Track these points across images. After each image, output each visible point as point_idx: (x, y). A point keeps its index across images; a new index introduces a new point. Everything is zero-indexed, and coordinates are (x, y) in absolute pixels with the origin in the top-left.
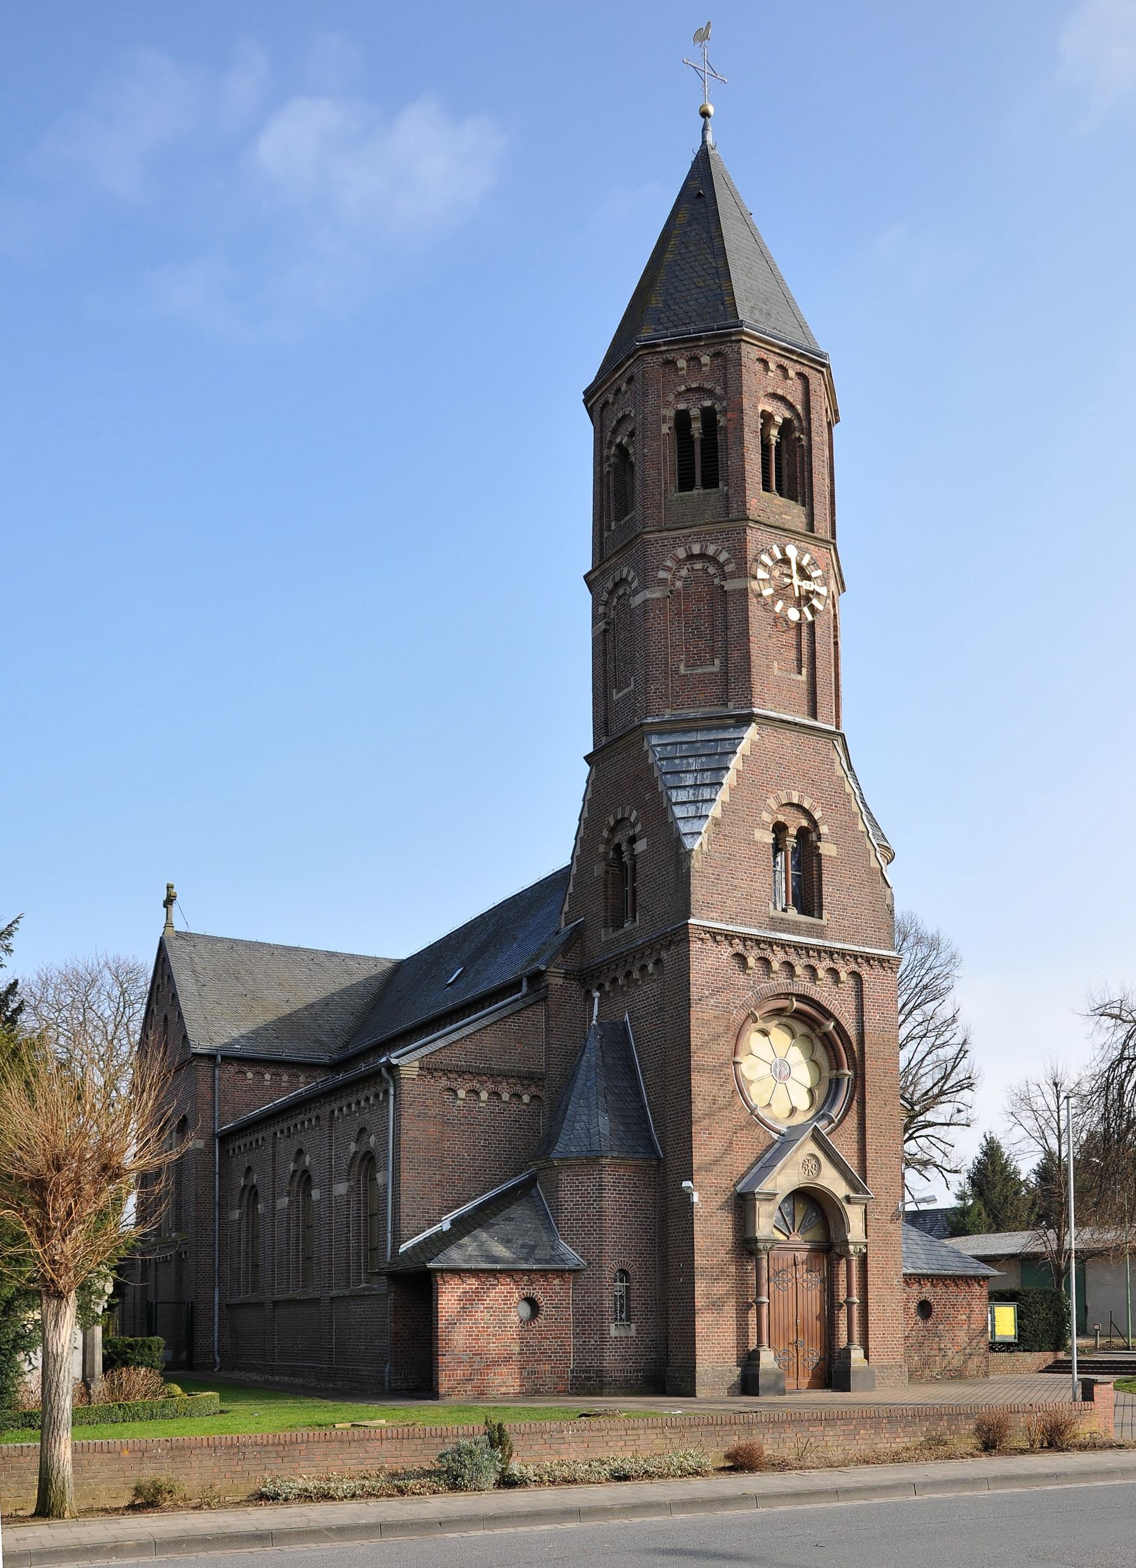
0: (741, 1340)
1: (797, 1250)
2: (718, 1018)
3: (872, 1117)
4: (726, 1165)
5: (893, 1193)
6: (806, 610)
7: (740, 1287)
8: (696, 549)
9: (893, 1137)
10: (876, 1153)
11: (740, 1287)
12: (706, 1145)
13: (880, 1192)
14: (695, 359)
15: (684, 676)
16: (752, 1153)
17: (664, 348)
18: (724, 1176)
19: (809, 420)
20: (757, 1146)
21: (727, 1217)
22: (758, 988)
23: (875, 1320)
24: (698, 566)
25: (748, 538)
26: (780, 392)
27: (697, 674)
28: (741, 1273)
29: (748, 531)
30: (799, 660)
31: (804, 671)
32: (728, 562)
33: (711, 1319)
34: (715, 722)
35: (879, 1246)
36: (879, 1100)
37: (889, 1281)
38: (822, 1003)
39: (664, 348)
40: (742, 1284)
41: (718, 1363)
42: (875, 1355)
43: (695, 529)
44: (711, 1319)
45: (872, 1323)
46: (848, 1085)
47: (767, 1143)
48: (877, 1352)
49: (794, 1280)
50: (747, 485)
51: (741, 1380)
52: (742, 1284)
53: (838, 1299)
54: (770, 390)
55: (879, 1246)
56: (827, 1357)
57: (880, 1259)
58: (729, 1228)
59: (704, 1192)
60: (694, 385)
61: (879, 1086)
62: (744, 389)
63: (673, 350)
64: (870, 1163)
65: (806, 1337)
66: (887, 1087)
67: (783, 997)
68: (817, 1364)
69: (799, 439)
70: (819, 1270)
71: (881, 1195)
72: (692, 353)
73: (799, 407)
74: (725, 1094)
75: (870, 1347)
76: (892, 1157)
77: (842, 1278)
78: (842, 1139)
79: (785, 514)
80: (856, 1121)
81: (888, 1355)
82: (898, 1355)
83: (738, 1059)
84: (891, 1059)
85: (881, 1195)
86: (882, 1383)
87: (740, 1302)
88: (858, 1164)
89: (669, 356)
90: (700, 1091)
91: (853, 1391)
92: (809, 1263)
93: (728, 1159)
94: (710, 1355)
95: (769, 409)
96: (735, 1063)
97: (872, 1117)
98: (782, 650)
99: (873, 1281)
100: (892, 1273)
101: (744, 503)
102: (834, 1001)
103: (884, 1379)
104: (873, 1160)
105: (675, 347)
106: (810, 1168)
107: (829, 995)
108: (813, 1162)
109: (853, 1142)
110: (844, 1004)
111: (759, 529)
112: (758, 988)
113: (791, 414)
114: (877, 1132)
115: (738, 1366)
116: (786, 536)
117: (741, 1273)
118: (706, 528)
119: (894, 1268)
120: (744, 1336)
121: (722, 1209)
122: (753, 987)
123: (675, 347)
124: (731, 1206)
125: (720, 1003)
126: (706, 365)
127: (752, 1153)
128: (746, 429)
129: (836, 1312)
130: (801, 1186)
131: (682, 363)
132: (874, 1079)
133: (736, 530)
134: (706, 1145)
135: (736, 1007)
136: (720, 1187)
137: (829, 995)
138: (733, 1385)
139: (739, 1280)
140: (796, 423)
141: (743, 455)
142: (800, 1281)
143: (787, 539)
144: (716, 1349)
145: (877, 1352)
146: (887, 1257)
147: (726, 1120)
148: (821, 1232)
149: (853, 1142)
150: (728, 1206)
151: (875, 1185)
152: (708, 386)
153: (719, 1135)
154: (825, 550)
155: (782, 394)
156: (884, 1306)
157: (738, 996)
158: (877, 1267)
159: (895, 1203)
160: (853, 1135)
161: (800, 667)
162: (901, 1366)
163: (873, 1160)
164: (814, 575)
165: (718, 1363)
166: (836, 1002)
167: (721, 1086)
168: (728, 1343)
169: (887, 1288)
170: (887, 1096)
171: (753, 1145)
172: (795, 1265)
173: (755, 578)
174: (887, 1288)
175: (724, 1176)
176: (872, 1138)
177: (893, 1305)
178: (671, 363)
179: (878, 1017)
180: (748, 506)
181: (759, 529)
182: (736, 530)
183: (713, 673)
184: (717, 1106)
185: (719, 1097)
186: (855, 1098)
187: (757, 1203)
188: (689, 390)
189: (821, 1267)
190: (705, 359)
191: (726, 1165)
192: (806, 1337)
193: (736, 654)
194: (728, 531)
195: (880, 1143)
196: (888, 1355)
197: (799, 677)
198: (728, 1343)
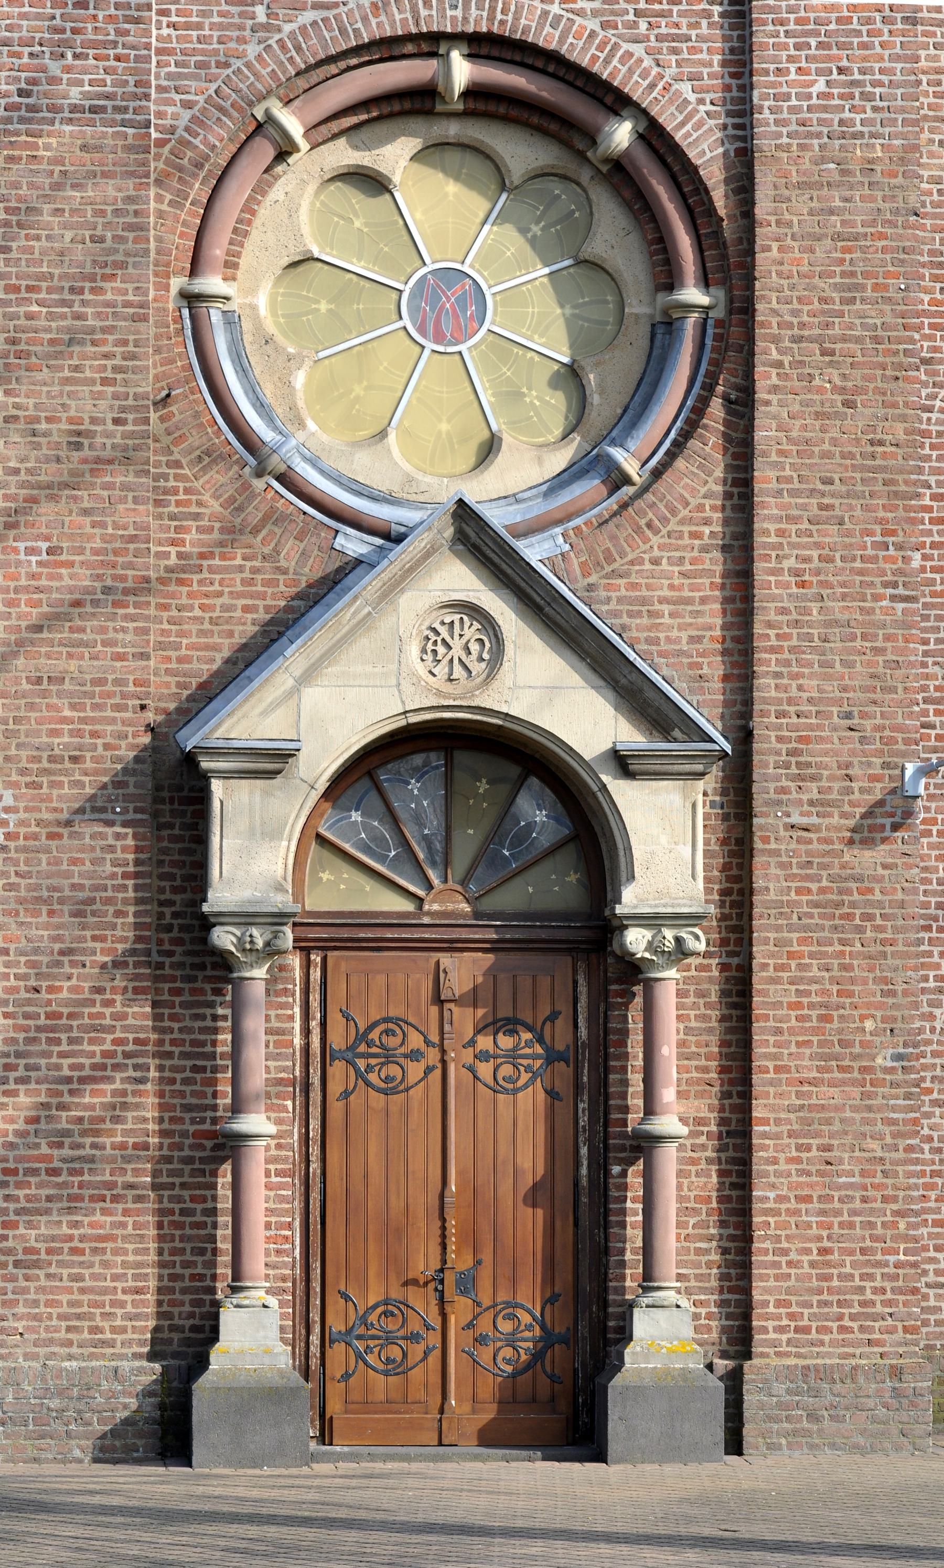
0: (186, 1265)
1: (452, 946)
2: (98, 149)
3: (781, 453)
4: (120, 657)
5: (878, 728)
7: (185, 1081)
9: (880, 521)
10: (802, 585)
11: (185, 1081)
12: (38, 590)
13: (820, 727)
16: (246, 609)
18: (110, 695)
20: (267, 583)
21: (118, 836)
22: (287, 28)
23: (780, 1199)
28: (190, 1030)
33: (45, 1192)
35: (806, 928)
36: (820, 390)
37: (854, 1057)
38: (574, 57)
40: (196, 1069)
41: (70, 1343)
42: (781, 1329)
44: (45, 1192)
45: (766, 1212)
46: (700, 346)
47: (313, 570)
48: (792, 1316)
49: (433, 1056)
51: (162, 1407)
52: (196, 1069)
53: (624, 1123)
55: (806, 928)
56: (583, 1330)
57: (815, 972)
58: (125, 876)
59: (24, 754)
61: (819, 340)
64: (770, 625)
65: (487, 1256)
66: (858, 340)
67: (410, 48)
68: (537, 1356)
70: (553, 1017)
71: (821, 740)
74: (123, 409)
75: (757, 1296)
76: (877, 598)
77: (636, 1046)
78: (655, 540)
80: (719, 473)
81: (843, 1329)
82: (891, 1331)
83: (211, 283)
84: (882, 236)
85: (821, 740)
86: (807, 1433)
87: (184, 1134)
88: (724, 627)
90: (17, 406)
91: (619, 1461)
92: (505, 993)
93: (129, 637)
94: (37, 1318)
96: (192, 299)
97: (781, 453)
99: (775, 1057)
100: (869, 1025)
102: (625, 46)
103: (813, 1417)
104: (784, 611)
106: (457, 651)
107: (604, 26)
108: (472, 631)
109: (704, 549)
110: (675, 51)
112: (287, 28)
114: (804, 507)
115: (152, 1356)
117: (190, 1030)
119: (880, 1006)
120: (202, 1252)
121: (103, 810)
122: (266, 27)
124: (138, 798)
125: (107, 97)
127: (246, 609)
129: (616, 1169)
130: (414, 719)
132: (795, 313)
134: (38, 590)
135: (187, 105)
136: (94, 734)
137: (604, 26)
138: (126, 1422)
139: (185, 1055)
142: (460, 1058)
144: (64, 1298)
145: (792, 1316)
146: (845, 968)
147: (124, 500)
148: (573, 878)
149: (704, 549)
150: (127, 798)
151: (790, 701)
153: (96, 552)
156: (828, 1148)
157: (199, 65)
158: (799, 1006)
159: (885, 766)
160: (707, 522)
162: (897, 1373)
163: (784, 611)
165: (70, 1343)
166: (638, 50)
167: (105, 382)
168: (115, 1278)
169: (843, 1083)
170: (857, 373)
171: (250, 582)
172: (439, 1001)
174: (843, 1083)
175: (110, 695)
176: (781, 533)
177: (874, 1145)
179: (820, 86)
184: (86, 453)
185: (93, 421)
186: (720, 389)
187: (217, 786)
189: (564, 1007)
191: (120, 657)
192: (487, 1256)
195: (817, 545)
196: (843, 1329)
198: (115, 1278)
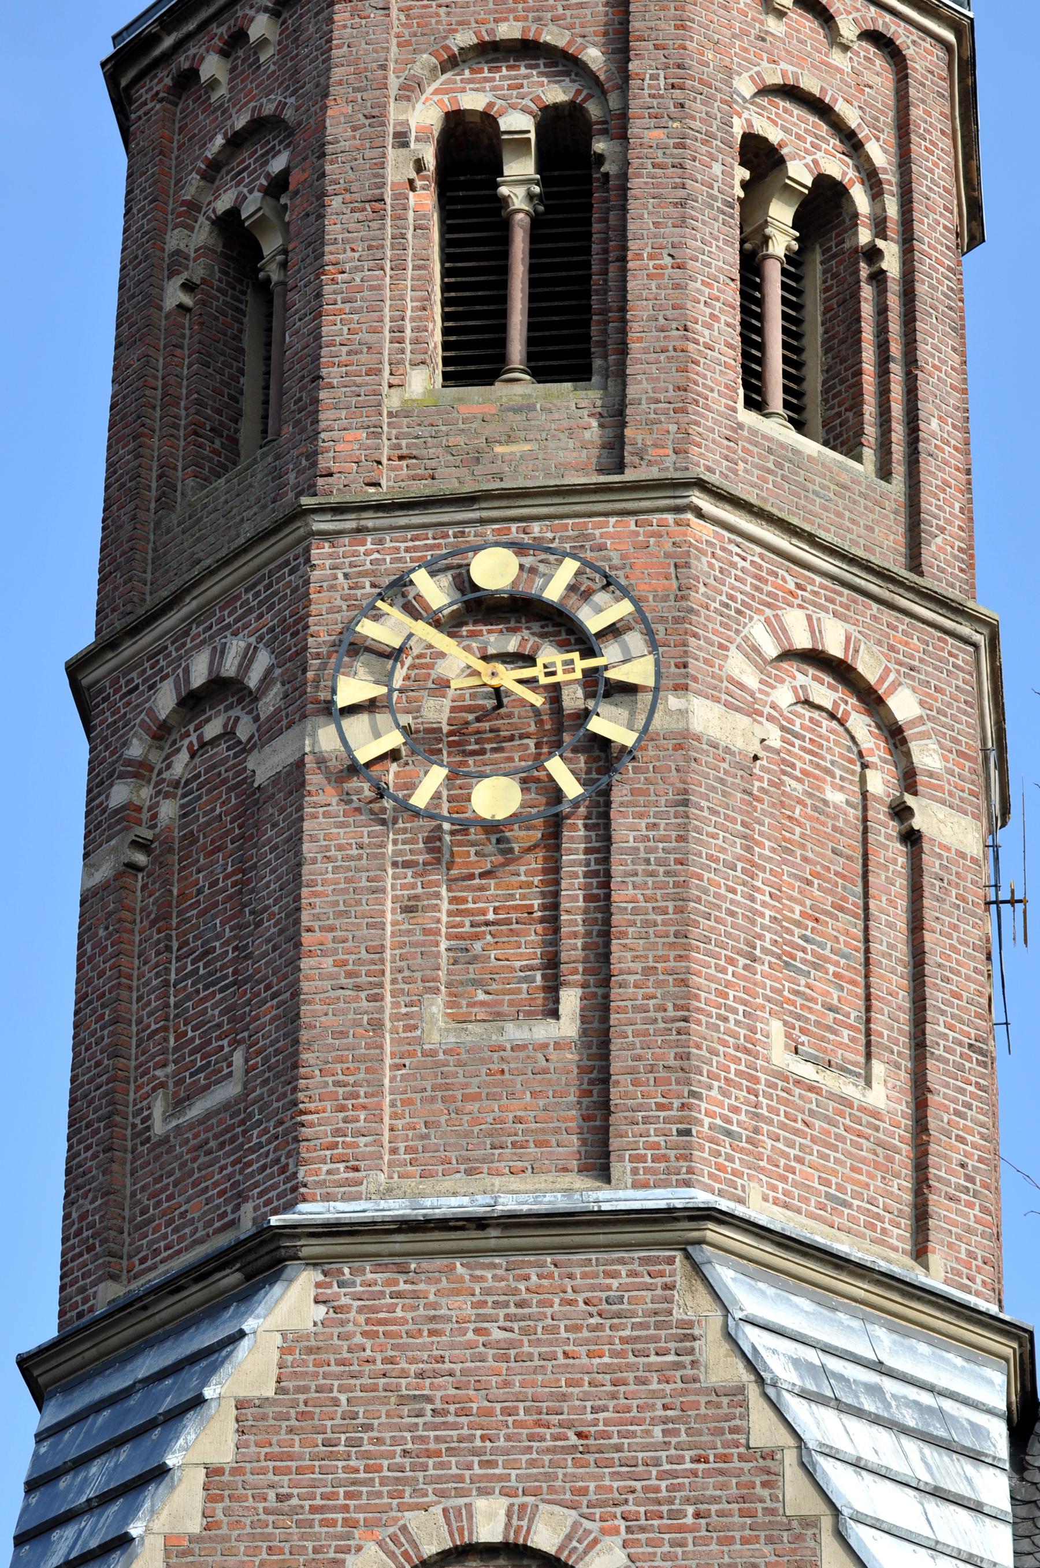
6: (558, 768)
8: (199, 674)
14: (239, 37)
15: (165, 1140)
17: (168, 42)
19: (624, 76)
24: (213, 729)
25: (315, 575)
26: (508, 30)
27: (191, 1126)
29: (321, 552)
30: (552, 963)
31: (570, 1000)
32: (267, 679)
34: (195, 1294)
39: (168, 42)
43: (189, 606)
50: (322, 395)
54: (465, 38)
60: (240, 122)
62: (338, 73)
63: (189, 36)
69: (600, 158)
72: (232, 22)
73: (594, 56)
79: (510, 440)
89: (183, 62)
95: (473, 101)
98: (478, 946)
101: (312, 456)
105: (191, 26)
111: (358, 530)
113: (576, 86)
116: (482, 521)
118: (213, 588)
123: (191, 26)
126: (263, 42)
128: (335, 203)
131: (212, 67)
133: (287, 563)
140: (594, 110)
141: (319, 295)
143: (489, 529)
152: (268, 109)
154: (670, 517)
155: (517, 35)
161: (553, 988)
164: (593, 622)
173: (328, 710)
178: (188, 79)
180: (324, 462)
181: (358, 530)
182: (287, 563)
183: (226, 1107)
188: (236, 142)
190: (260, 27)
193: (269, 1012)
194: (271, 574)
197: (544, 1031)
